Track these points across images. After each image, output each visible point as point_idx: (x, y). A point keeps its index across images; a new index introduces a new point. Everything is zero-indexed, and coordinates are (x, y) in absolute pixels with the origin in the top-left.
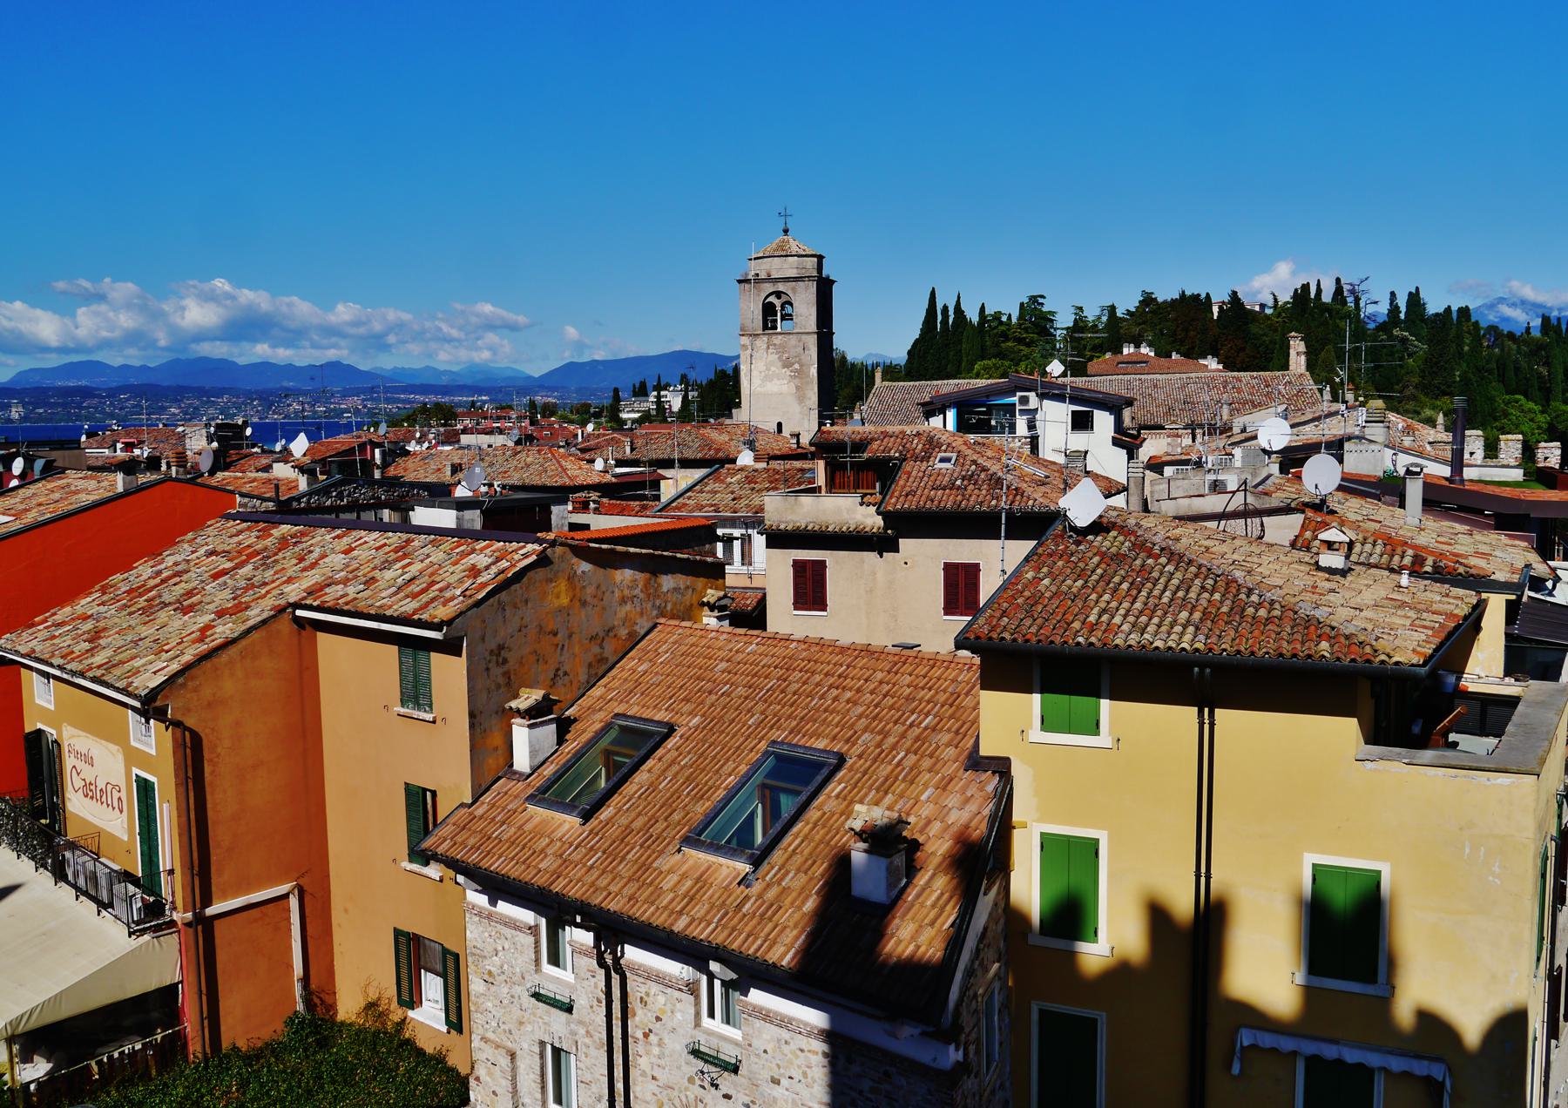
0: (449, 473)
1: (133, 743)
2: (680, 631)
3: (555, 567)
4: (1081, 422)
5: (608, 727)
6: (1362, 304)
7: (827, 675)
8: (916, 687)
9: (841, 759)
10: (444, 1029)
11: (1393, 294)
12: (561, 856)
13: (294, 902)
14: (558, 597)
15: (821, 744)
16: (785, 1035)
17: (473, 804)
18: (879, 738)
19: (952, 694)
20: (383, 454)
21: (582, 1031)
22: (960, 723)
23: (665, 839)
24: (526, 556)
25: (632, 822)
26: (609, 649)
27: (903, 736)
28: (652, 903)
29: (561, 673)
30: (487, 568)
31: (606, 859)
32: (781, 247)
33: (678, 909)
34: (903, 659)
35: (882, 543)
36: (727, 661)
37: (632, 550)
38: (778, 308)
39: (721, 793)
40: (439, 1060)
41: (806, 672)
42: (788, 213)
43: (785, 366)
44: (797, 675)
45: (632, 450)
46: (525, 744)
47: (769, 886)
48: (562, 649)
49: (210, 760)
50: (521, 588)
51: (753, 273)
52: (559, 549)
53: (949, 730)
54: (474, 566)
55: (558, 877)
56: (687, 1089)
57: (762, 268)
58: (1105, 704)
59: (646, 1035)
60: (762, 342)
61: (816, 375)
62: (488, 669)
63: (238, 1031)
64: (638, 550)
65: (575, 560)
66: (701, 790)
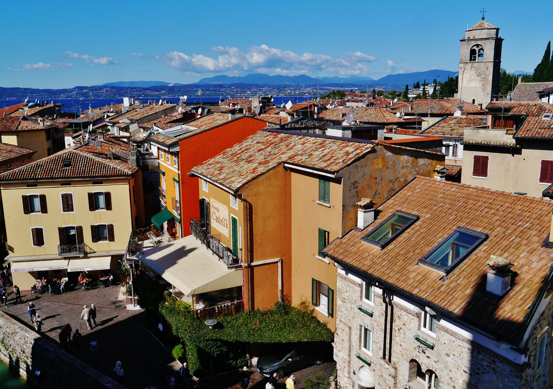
0: (341, 117)
1: (231, 206)
2: (425, 181)
3: (377, 153)
5: (394, 215)
7: (484, 202)
8: (523, 211)
9: (487, 237)
10: (327, 315)
12: (372, 260)
13: (279, 264)
14: (378, 165)
15: (479, 230)
16: (453, 339)
17: (342, 238)
18: (504, 230)
19: (539, 215)
20: (318, 109)
21: (376, 324)
22: (541, 227)
23: (412, 259)
24: (367, 148)
25: (400, 251)
27: (515, 230)
28: (405, 282)
29: (377, 193)
30: (352, 152)
31: (389, 263)
32: (480, 26)
33: (415, 285)
34: (518, 199)
35: (514, 151)
36: (443, 194)
37: (408, 148)
38: (477, 52)
39: (436, 245)
40: (324, 326)
41: (475, 201)
42: (485, 10)
43: (478, 76)
44: (472, 201)
45: (411, 110)
47: (452, 282)
48: (378, 184)
49: (255, 214)
50: (364, 160)
51: (467, 37)
52: (379, 147)
53: (536, 230)
54: (347, 151)
55: (371, 268)
56: (413, 352)
57: (471, 35)
59: (399, 330)
60: (469, 66)
61: (491, 79)
62: (350, 190)
64: (410, 148)
65: (385, 151)
66: (428, 242)
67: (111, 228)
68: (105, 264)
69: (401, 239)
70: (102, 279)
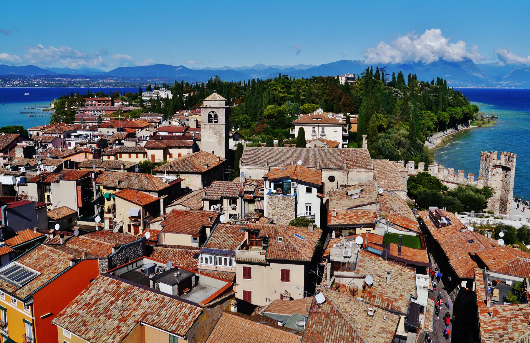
0: (117, 183)
4: (309, 190)
6: (384, 75)
11: (394, 73)
20: (95, 174)
26: (213, 325)
38: (213, 116)
43: (215, 134)
45: (171, 168)
54: (185, 314)
60: (208, 127)
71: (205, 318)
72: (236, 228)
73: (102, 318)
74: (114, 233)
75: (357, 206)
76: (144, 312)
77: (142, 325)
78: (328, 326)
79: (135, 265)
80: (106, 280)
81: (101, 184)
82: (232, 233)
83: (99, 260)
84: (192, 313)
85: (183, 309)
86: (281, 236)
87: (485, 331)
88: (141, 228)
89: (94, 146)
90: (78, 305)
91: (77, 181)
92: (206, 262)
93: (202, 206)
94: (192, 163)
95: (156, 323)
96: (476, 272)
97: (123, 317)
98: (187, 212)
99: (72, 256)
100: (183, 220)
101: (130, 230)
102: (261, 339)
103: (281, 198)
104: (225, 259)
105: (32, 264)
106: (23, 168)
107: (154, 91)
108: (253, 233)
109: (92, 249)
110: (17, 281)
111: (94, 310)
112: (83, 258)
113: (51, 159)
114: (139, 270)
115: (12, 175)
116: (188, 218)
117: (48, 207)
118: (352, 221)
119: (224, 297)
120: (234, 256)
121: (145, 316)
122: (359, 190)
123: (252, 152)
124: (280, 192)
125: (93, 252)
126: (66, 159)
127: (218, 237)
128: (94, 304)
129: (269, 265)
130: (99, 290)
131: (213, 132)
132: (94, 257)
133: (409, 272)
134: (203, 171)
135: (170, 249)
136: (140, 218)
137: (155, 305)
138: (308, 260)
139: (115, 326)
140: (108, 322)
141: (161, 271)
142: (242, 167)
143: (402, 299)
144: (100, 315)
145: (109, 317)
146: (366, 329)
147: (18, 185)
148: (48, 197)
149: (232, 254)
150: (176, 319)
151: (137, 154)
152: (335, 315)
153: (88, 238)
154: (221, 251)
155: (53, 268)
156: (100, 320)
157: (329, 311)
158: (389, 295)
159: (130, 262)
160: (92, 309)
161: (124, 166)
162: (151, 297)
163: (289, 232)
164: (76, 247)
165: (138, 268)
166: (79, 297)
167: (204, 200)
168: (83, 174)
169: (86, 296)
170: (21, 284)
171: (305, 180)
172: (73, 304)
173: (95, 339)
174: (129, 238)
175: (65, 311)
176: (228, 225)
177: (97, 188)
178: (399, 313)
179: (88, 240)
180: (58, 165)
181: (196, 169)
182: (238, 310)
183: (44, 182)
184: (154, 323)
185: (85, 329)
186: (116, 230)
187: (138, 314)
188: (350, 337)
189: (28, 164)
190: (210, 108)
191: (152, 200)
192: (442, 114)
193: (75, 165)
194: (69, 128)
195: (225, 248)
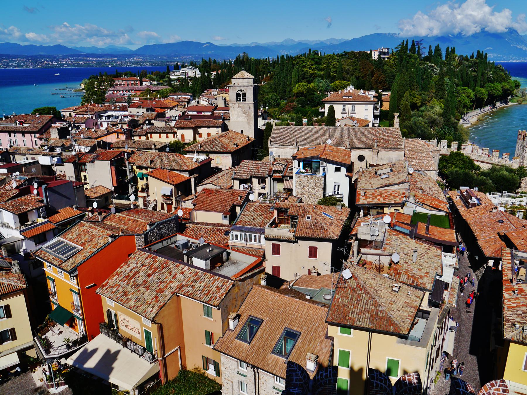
0: (149, 163)
4: (337, 170)
6: (420, 48)
11: (430, 46)
13: (179, 350)
15: (295, 328)
17: (223, 336)
20: (127, 155)
27: (312, 328)
38: (241, 95)
40: (214, 381)
45: (201, 147)
46: (232, 325)
54: (217, 287)
58: (352, 330)
60: (236, 105)
63: (171, 377)
67: (13, 330)
68: (15, 359)
69: (257, 337)
70: (12, 372)
71: (237, 291)
72: (265, 206)
73: (141, 289)
74: (148, 211)
75: (386, 186)
76: (179, 284)
77: (178, 296)
78: (354, 300)
79: (169, 241)
80: (143, 255)
81: (134, 163)
82: (262, 212)
83: (135, 236)
84: (224, 286)
85: (216, 282)
86: (310, 215)
87: (508, 308)
88: (173, 206)
89: (125, 126)
90: (118, 277)
91: (111, 161)
92: (237, 239)
93: (231, 186)
94: (222, 143)
95: (191, 294)
96: (504, 252)
97: (160, 289)
98: (217, 191)
99: (110, 233)
100: (214, 199)
101: (163, 208)
102: (290, 310)
103: (310, 177)
104: (255, 236)
105: (74, 239)
106: (59, 148)
107: (182, 69)
108: (282, 211)
109: (129, 226)
110: (62, 254)
111: (134, 282)
112: (121, 234)
113: (85, 140)
114: (173, 246)
115: (49, 155)
116: (218, 196)
117: (85, 186)
118: (381, 200)
119: (254, 272)
120: (263, 233)
121: (180, 287)
122: (388, 170)
123: (281, 132)
124: (309, 172)
125: (130, 228)
126: (99, 140)
127: (248, 215)
128: (133, 276)
129: (297, 242)
130: (137, 264)
131: (242, 110)
132: (130, 233)
133: (436, 251)
134: (233, 150)
135: (202, 226)
136: (172, 197)
137: (190, 278)
138: (336, 237)
139: (153, 296)
140: (147, 293)
141: (194, 247)
142: (271, 146)
143: (427, 276)
144: (139, 287)
145: (147, 288)
146: (390, 303)
147: (56, 165)
148: (85, 176)
149: (261, 231)
150: (209, 291)
151: (167, 133)
152: (361, 290)
153: (124, 216)
154: (251, 228)
155: (94, 243)
156: (139, 291)
157: (355, 286)
158: (414, 272)
159: (164, 238)
160: (132, 281)
161: (155, 146)
162: (185, 271)
163: (318, 210)
164: (114, 224)
165: (172, 243)
166: (119, 270)
167: (234, 179)
168: (116, 155)
169: (126, 269)
170: (66, 257)
171: (334, 160)
172: (114, 276)
173: (135, 307)
174: (163, 216)
175: (108, 282)
176: (258, 204)
177: (130, 168)
178: (423, 289)
179: (124, 217)
180: (92, 145)
181: (225, 149)
182: (268, 284)
183: (79, 162)
184: (189, 294)
185: (126, 298)
186: (150, 208)
187: (174, 286)
188: (375, 310)
189: (63, 145)
190: (238, 86)
191: (183, 180)
192: (480, 90)
193: (107, 145)
194: (100, 109)
195: (255, 225)
